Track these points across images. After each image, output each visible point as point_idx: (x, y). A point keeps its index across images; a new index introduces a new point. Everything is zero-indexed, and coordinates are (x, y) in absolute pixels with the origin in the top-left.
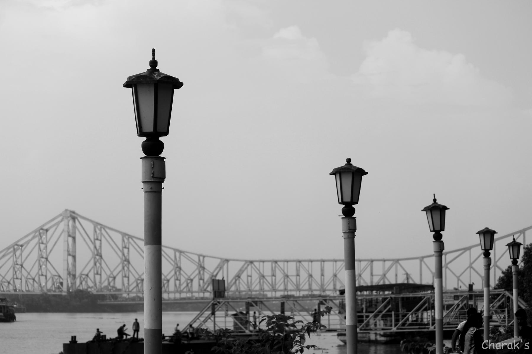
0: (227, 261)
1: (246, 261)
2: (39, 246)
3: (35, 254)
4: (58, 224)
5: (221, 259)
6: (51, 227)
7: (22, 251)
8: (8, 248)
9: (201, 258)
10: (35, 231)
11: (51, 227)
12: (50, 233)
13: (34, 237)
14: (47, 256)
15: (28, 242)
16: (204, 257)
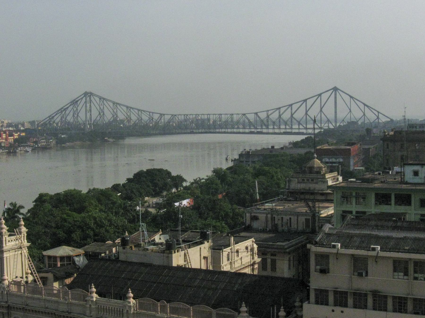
0: (164, 115)
1: (172, 115)
2: (73, 109)
3: (72, 114)
4: (82, 98)
6: (79, 100)
7: (66, 111)
8: (58, 111)
9: (151, 114)
10: (71, 102)
11: (79, 100)
12: (79, 103)
13: (70, 106)
14: (78, 113)
15: (68, 108)
16: (153, 113)
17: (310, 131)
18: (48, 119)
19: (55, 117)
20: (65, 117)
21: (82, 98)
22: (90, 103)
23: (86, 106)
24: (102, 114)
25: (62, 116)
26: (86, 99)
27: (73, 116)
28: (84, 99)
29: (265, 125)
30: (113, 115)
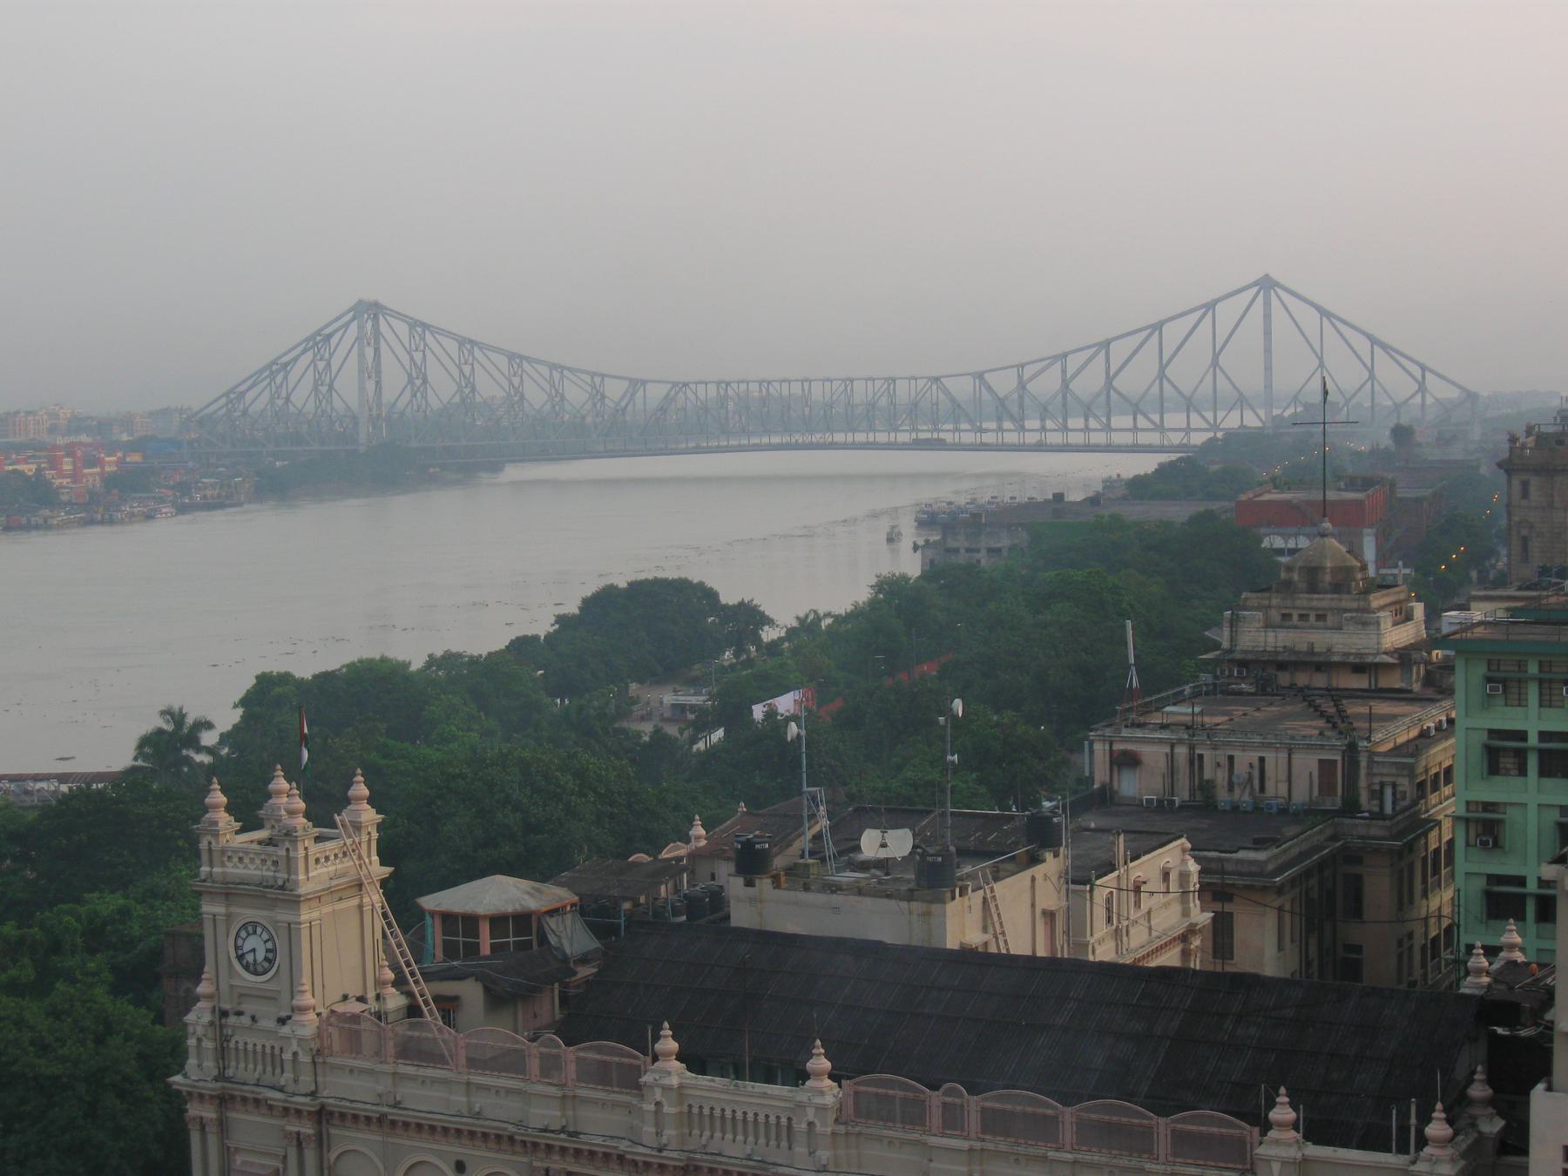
0: (644, 383)
1: (675, 384)
2: (315, 366)
4: (347, 325)
5: (630, 380)
6: (337, 331)
9: (597, 380)
10: (307, 340)
11: (337, 331)
12: (334, 340)
13: (304, 351)
15: (295, 360)
16: (603, 376)
17: (1176, 439)
18: (224, 400)
19: (250, 396)
20: (284, 394)
21: (347, 325)
22: (377, 342)
23: (361, 355)
24: (418, 382)
25: (274, 389)
26: (361, 328)
27: (315, 388)
28: (354, 325)
29: (1012, 418)
30: (459, 385)
